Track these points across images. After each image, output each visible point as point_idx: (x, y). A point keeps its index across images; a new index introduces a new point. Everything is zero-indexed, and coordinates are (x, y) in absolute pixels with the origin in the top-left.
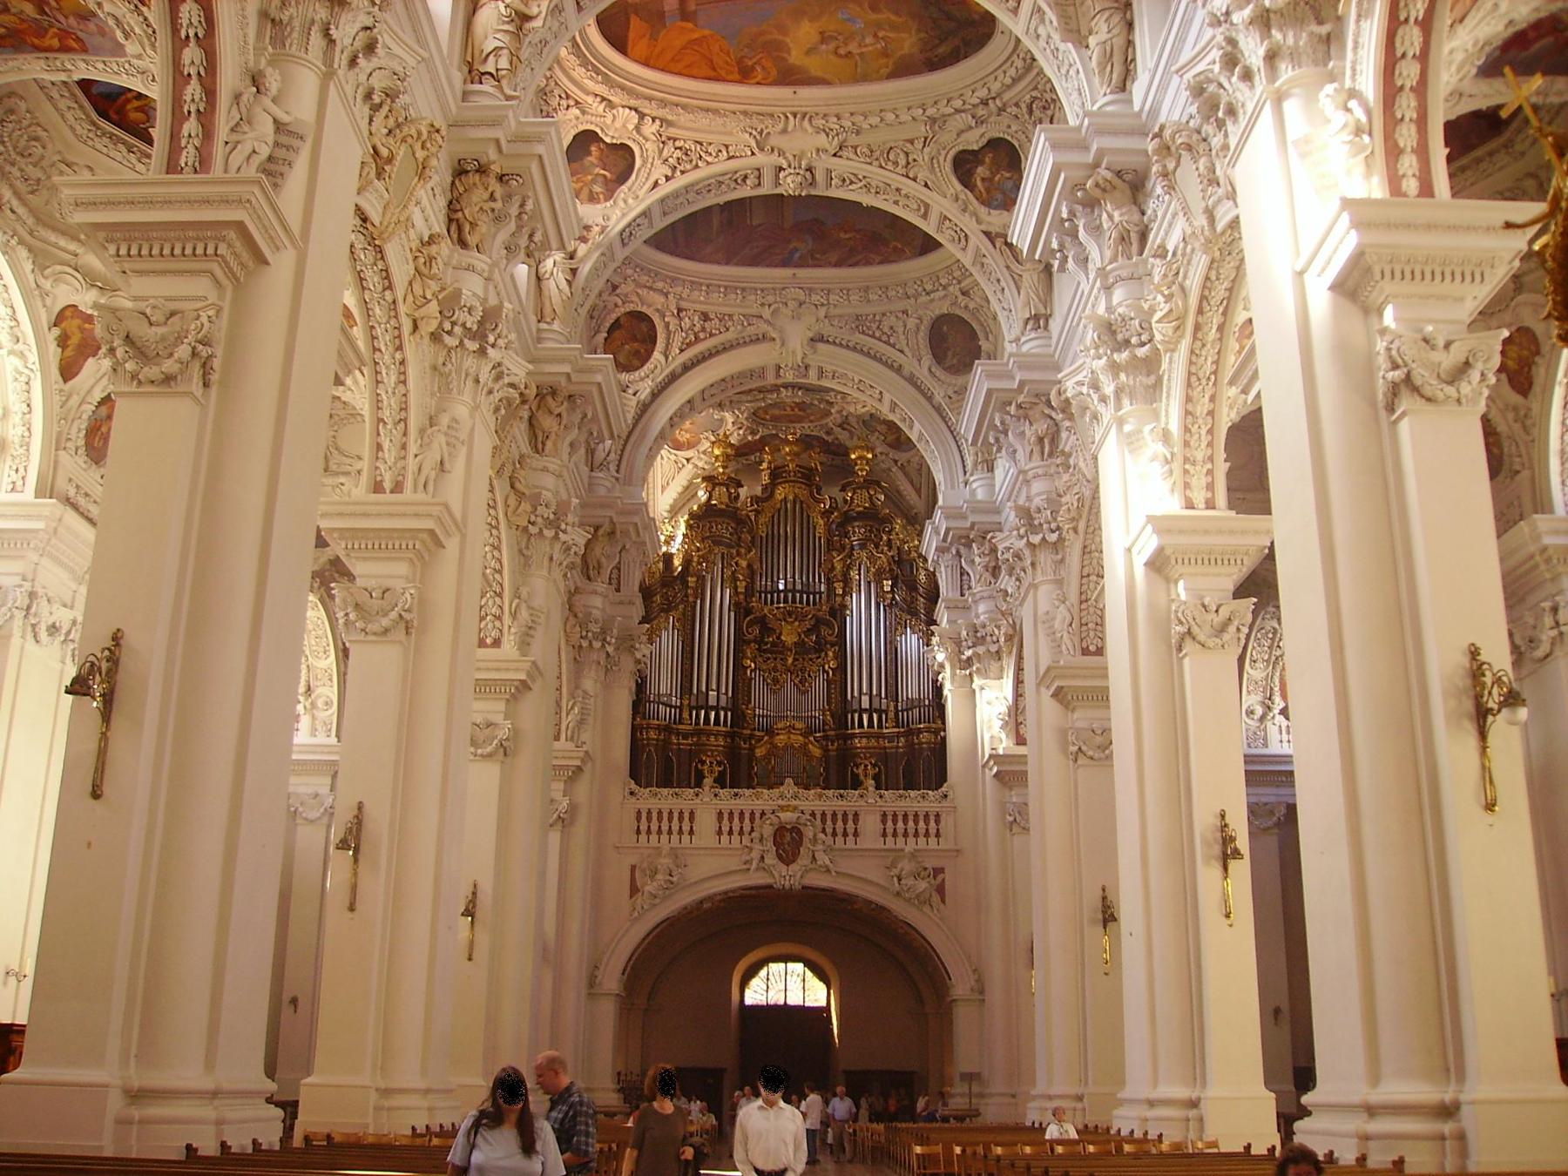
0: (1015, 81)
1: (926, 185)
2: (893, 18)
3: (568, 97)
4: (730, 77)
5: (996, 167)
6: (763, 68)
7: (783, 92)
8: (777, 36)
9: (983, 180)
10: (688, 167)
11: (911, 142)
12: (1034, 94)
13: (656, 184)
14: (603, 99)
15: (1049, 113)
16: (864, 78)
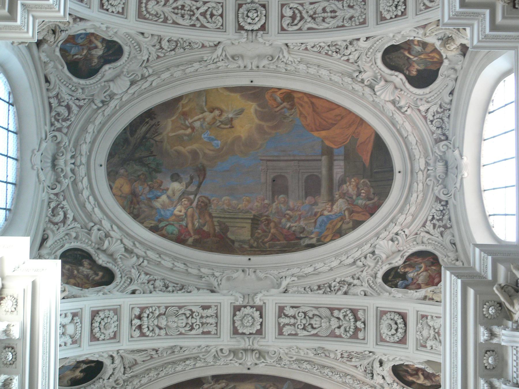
0: (84, 129)
1: (143, 34)
2: (180, 148)
3: (425, 118)
4: (300, 95)
5: (88, 59)
6: (275, 100)
7: (261, 82)
8: (265, 125)
9: (96, 47)
10: (339, 43)
11: (158, 57)
12: (69, 123)
13: (367, 38)
14: (400, 108)
15: (53, 114)
16: (199, 94)
